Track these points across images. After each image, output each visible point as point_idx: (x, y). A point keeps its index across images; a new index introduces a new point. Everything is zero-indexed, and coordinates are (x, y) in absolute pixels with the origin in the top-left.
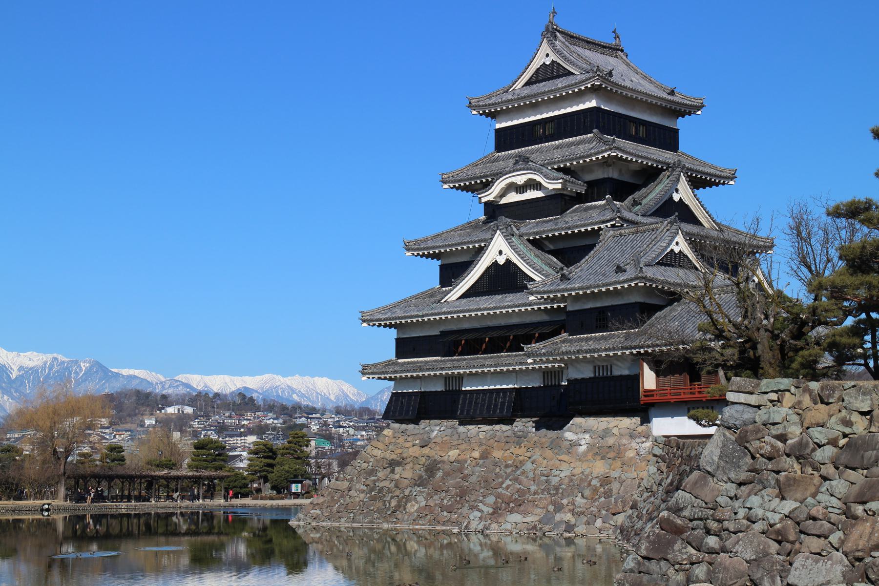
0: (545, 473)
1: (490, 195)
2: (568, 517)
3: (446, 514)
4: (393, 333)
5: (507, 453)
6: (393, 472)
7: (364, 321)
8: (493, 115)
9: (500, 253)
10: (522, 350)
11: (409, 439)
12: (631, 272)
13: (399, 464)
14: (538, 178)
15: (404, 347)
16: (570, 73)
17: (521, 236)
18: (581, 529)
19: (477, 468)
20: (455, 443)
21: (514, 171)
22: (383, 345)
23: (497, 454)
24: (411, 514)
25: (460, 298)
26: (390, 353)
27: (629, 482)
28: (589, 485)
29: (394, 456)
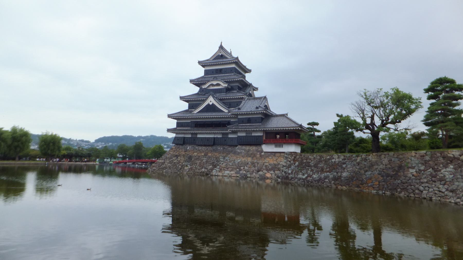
1: (204, 87)
2: (244, 172)
4: (176, 121)
5: (213, 155)
6: (177, 158)
8: (203, 66)
16: (227, 58)
18: (249, 175)
19: (204, 158)
22: (173, 124)
23: (210, 155)
24: (186, 170)
26: (174, 126)
27: (260, 163)
28: (248, 164)
29: (177, 154)
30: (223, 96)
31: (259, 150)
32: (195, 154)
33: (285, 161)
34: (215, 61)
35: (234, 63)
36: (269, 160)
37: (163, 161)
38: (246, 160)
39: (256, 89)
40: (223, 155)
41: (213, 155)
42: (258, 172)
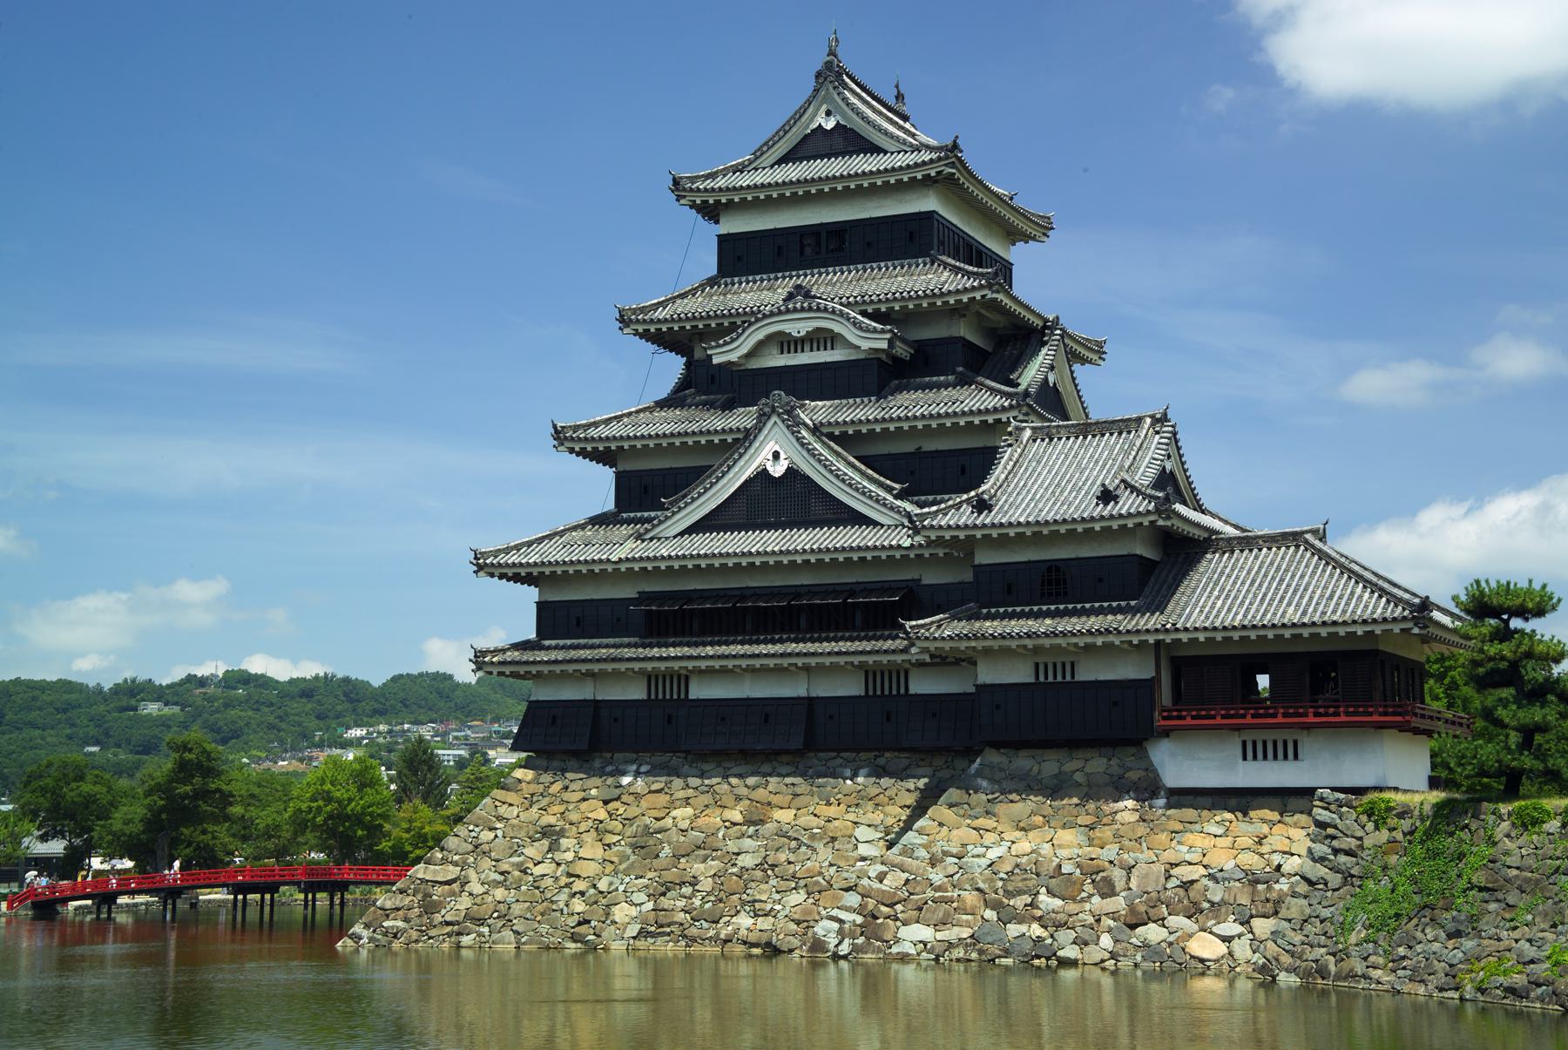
0: (954, 851)
2: (1036, 930)
3: (705, 925)
4: (531, 594)
7: (480, 568)
8: (711, 212)
9: (776, 456)
10: (903, 626)
11: (573, 786)
12: (1128, 503)
13: (562, 833)
14: (837, 328)
15: (552, 619)
17: (816, 430)
18: (1070, 952)
19: (748, 843)
20: (681, 794)
21: (788, 311)
22: (513, 615)
25: (682, 534)
29: (552, 820)
30: (860, 412)
31: (1133, 775)
32: (682, 814)
33: (1321, 849)
34: (793, 172)
35: (928, 181)
36: (1208, 842)
37: (452, 872)
38: (1046, 849)
39: (1081, 352)
40: (877, 817)
41: (806, 820)
42: (1133, 927)
